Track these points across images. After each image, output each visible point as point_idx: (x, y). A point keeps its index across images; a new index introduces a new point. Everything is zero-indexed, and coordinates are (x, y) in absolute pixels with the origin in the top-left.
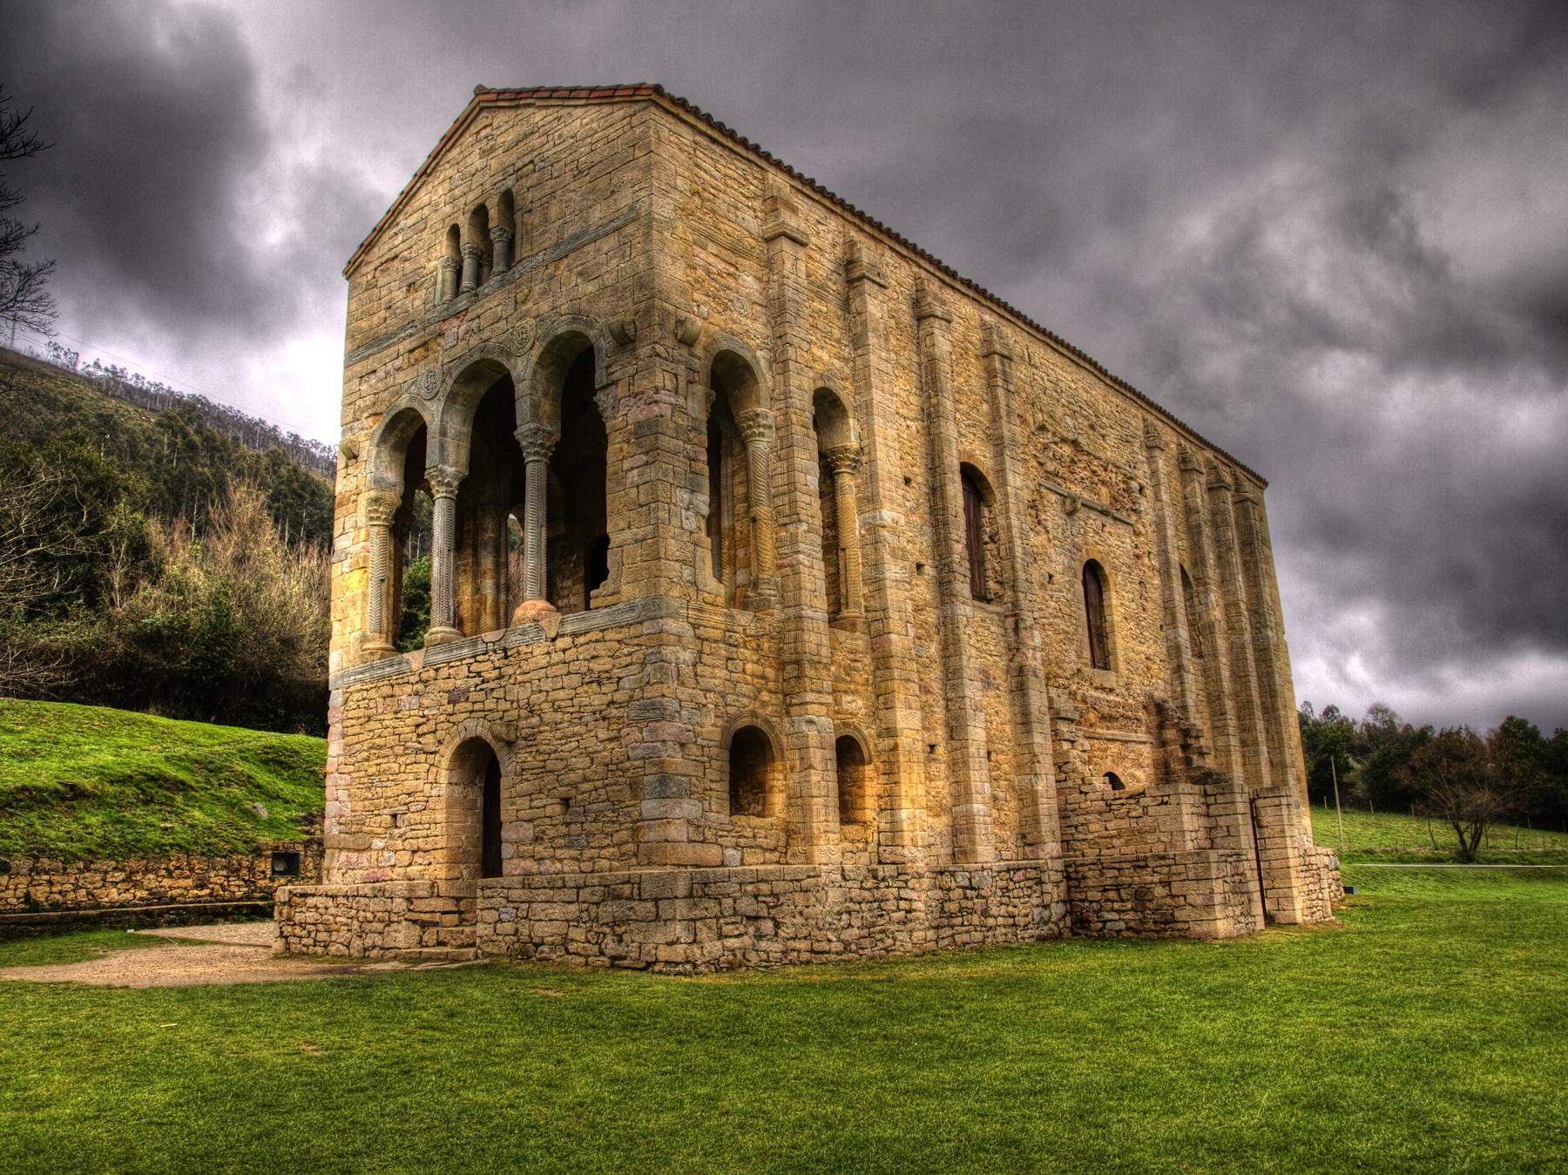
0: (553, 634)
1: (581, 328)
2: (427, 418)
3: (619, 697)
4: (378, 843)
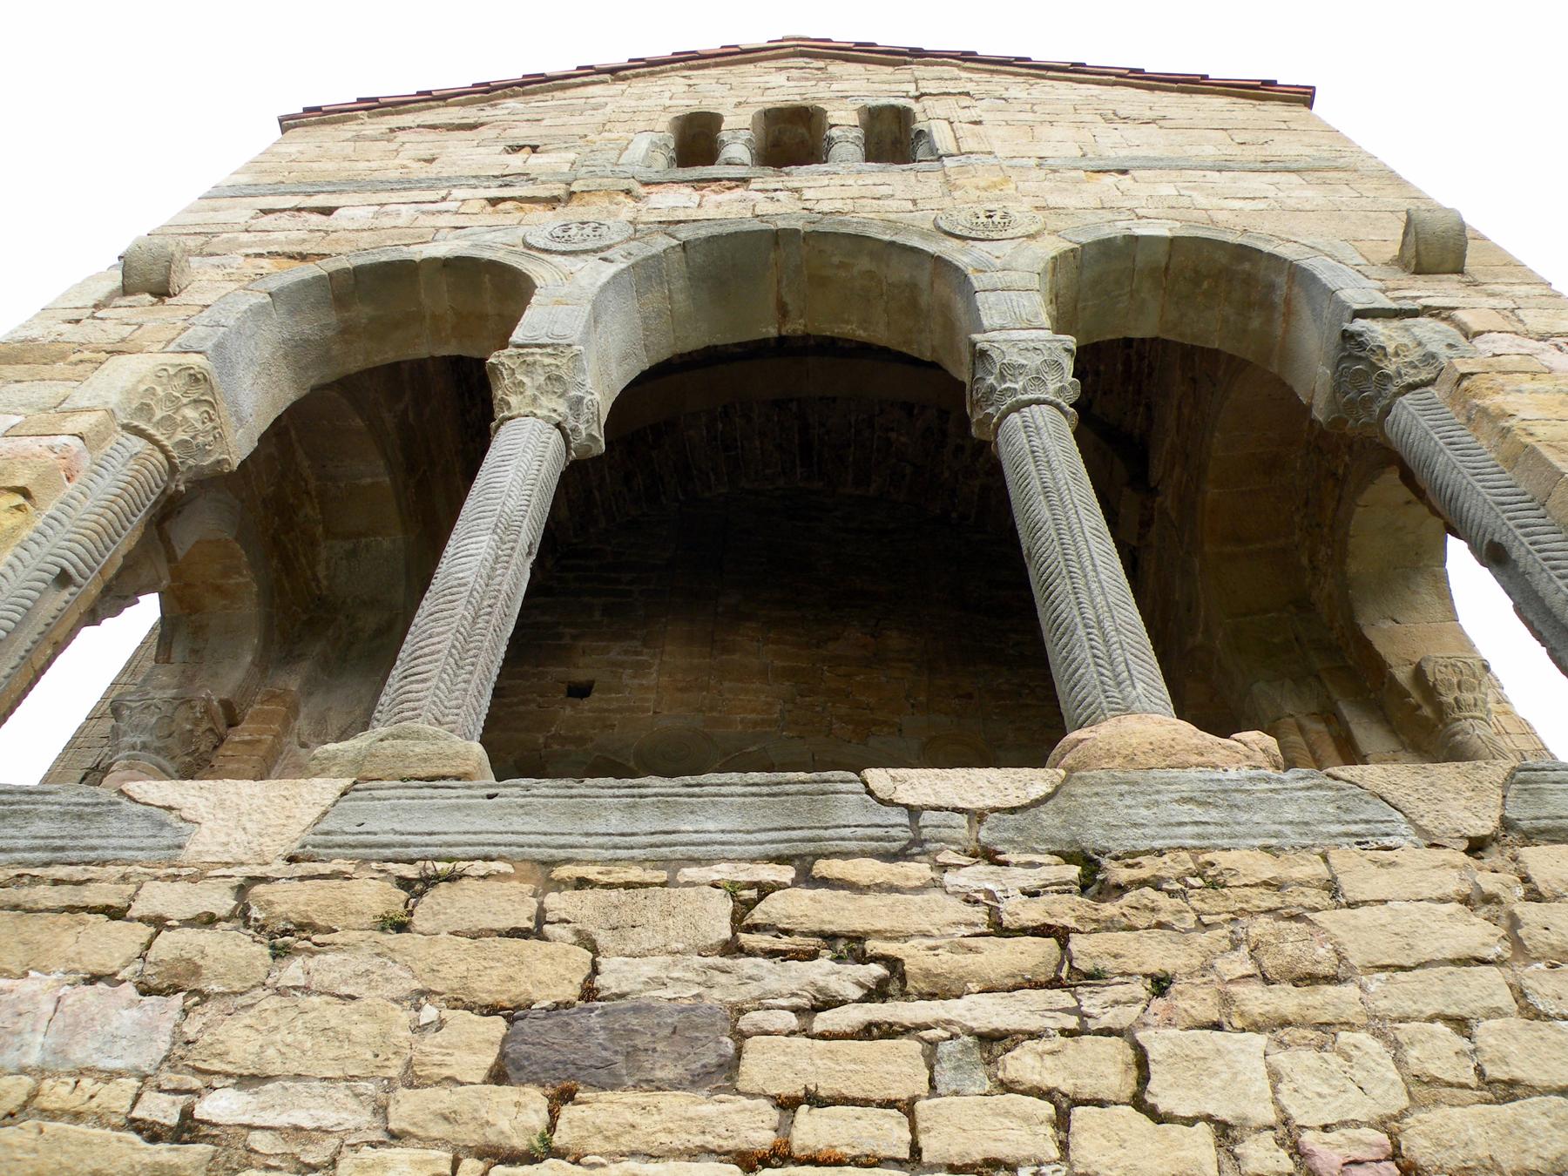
0: (1485, 825)
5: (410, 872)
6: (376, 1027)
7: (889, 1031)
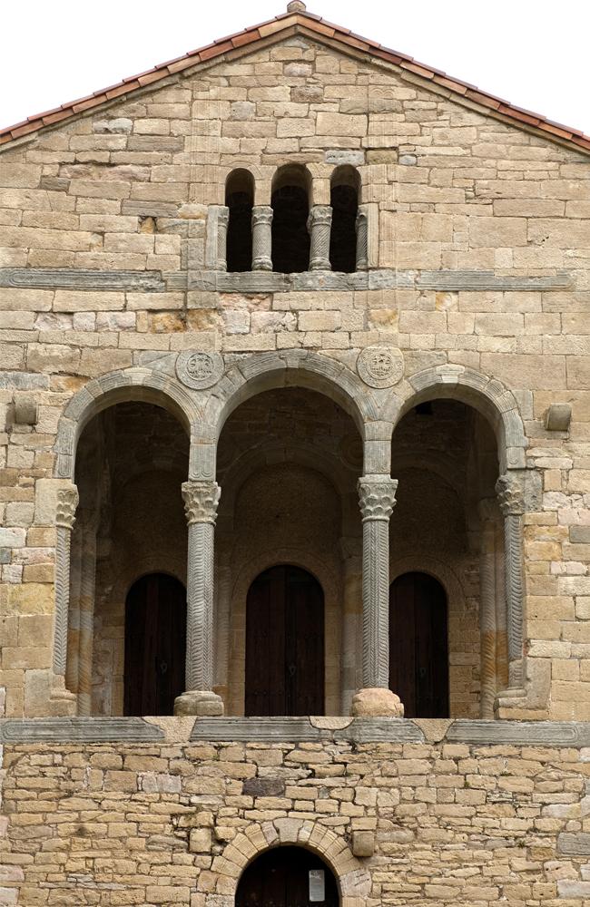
0: (439, 738)
1: (483, 388)
3: (541, 824)
5: (216, 744)
6: (217, 783)
7: (311, 786)
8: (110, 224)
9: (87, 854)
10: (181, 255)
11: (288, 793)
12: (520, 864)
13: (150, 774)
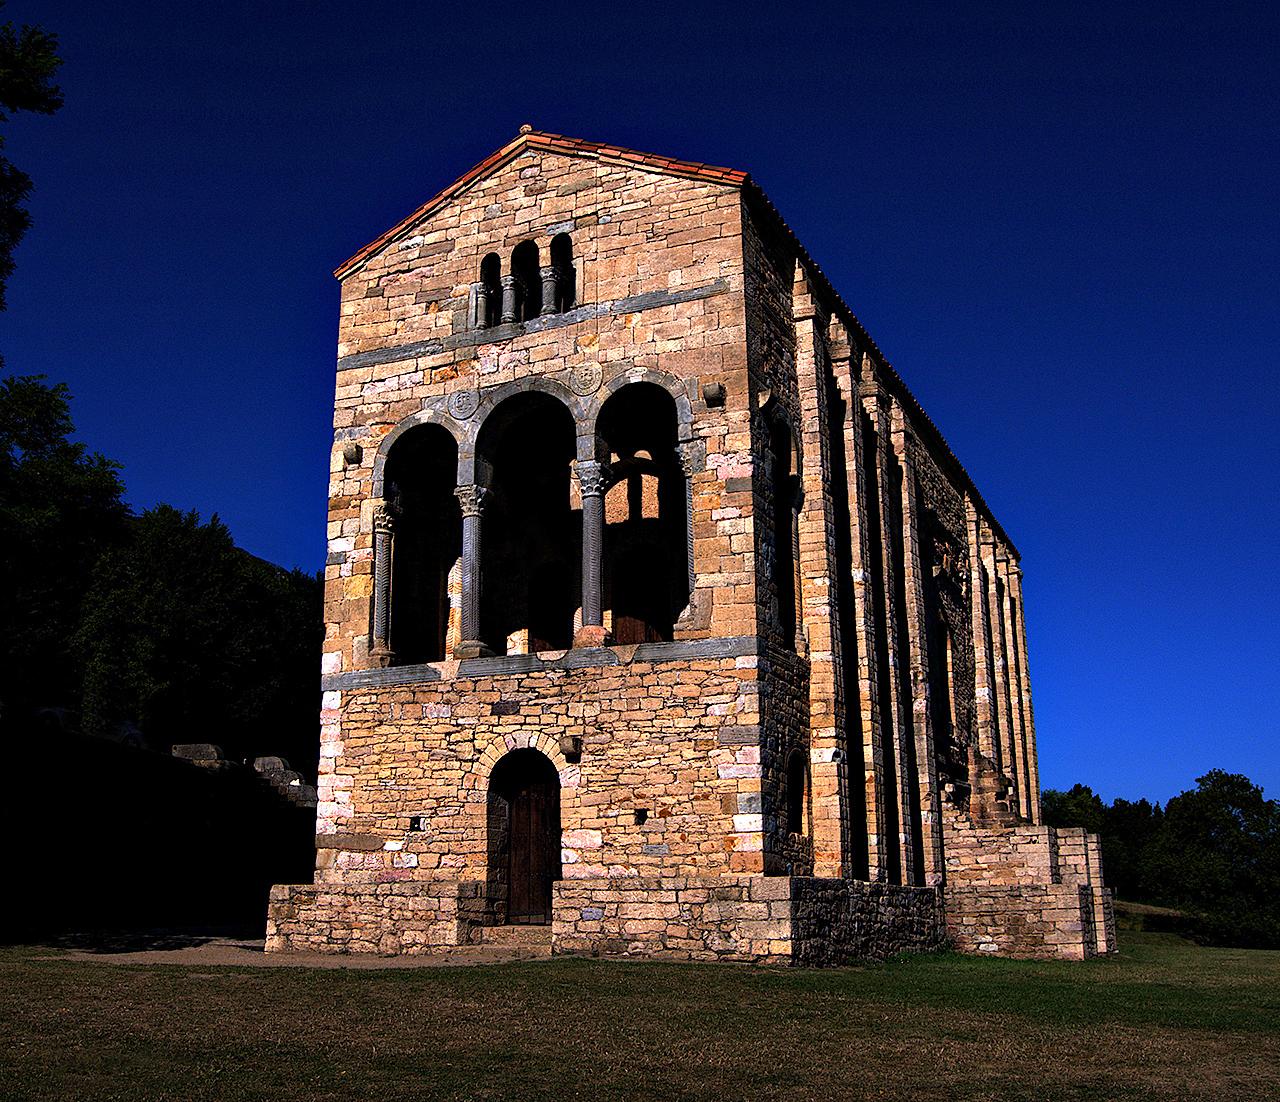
1: (660, 382)
2: (458, 437)
3: (706, 721)
4: (391, 845)
8: (409, 312)
9: (393, 765)
10: (452, 324)
11: (521, 712)
12: (689, 754)
13: (431, 704)
